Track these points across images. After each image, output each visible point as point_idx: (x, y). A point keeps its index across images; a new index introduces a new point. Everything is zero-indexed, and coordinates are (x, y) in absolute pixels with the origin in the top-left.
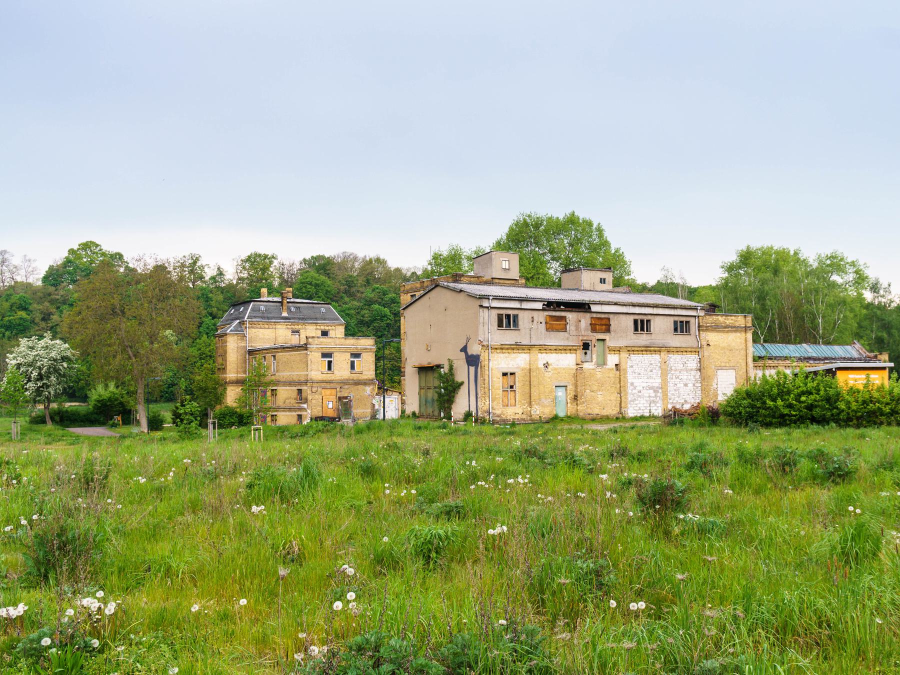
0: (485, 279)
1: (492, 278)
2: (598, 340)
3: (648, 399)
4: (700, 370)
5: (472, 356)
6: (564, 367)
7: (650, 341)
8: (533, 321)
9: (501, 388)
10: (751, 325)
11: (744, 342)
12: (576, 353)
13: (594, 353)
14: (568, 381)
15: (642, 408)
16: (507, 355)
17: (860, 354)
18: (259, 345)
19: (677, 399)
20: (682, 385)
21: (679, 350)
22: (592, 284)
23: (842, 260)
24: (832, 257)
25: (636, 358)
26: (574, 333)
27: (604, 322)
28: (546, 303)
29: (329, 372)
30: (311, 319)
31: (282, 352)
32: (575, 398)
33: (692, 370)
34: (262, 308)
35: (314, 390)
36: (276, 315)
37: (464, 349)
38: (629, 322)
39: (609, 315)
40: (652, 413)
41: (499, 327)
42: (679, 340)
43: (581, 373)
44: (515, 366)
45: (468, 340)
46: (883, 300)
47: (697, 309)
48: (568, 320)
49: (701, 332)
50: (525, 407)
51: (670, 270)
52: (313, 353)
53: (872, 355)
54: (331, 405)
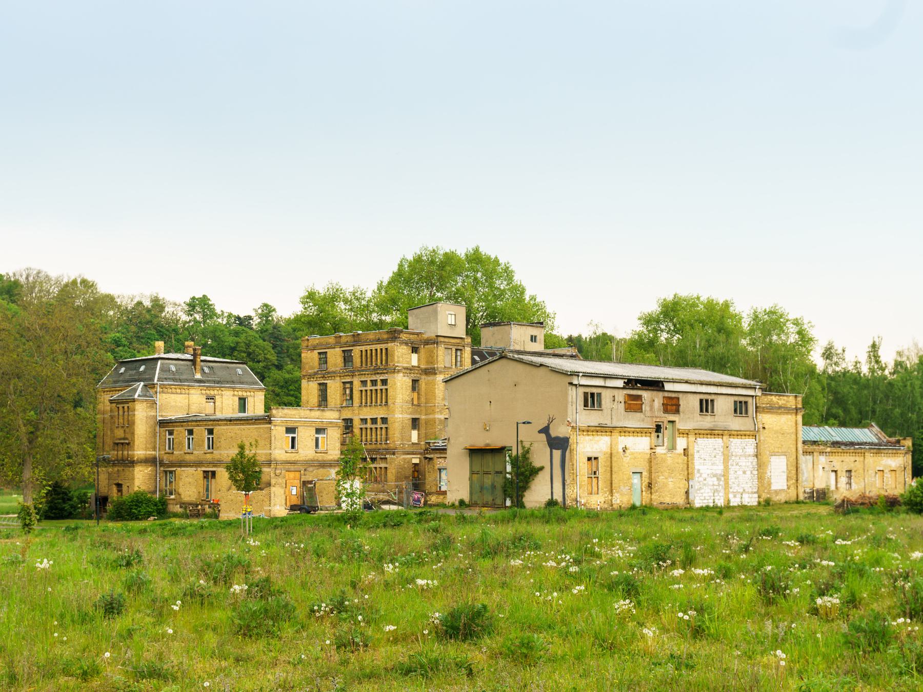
0: (425, 336)
1: (437, 336)
2: (669, 421)
3: (712, 487)
4: (757, 456)
5: (557, 438)
6: (640, 451)
7: (714, 423)
8: (614, 401)
9: (586, 474)
10: (801, 406)
11: (794, 425)
12: (650, 437)
13: (667, 433)
14: (643, 467)
15: (707, 498)
16: (591, 437)
17: (879, 439)
18: (172, 415)
19: (737, 488)
20: (741, 473)
21: (739, 434)
22: (523, 343)
23: (781, 316)
24: (771, 313)
25: (702, 441)
26: (648, 414)
27: (674, 402)
28: (626, 381)
29: (293, 450)
30: (228, 382)
31: (226, 425)
32: (650, 486)
33: (749, 455)
34: (173, 369)
35: (278, 472)
36: (190, 377)
37: (545, 430)
38: (694, 402)
39: (679, 394)
40: (715, 503)
41: (585, 406)
42: (737, 423)
43: (655, 459)
44: (599, 450)
45: (551, 421)
46: (837, 369)
47: (755, 388)
48: (643, 399)
49: (758, 414)
50: (606, 495)
51: (599, 325)
52: (277, 427)
53: (893, 439)
54: (294, 492)
